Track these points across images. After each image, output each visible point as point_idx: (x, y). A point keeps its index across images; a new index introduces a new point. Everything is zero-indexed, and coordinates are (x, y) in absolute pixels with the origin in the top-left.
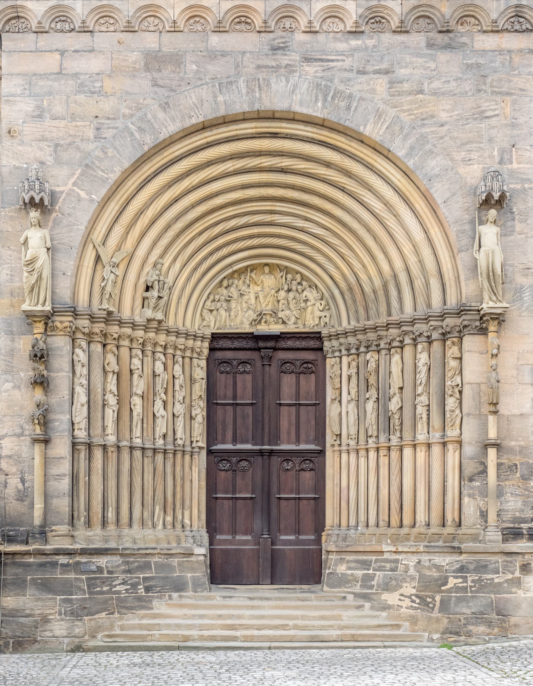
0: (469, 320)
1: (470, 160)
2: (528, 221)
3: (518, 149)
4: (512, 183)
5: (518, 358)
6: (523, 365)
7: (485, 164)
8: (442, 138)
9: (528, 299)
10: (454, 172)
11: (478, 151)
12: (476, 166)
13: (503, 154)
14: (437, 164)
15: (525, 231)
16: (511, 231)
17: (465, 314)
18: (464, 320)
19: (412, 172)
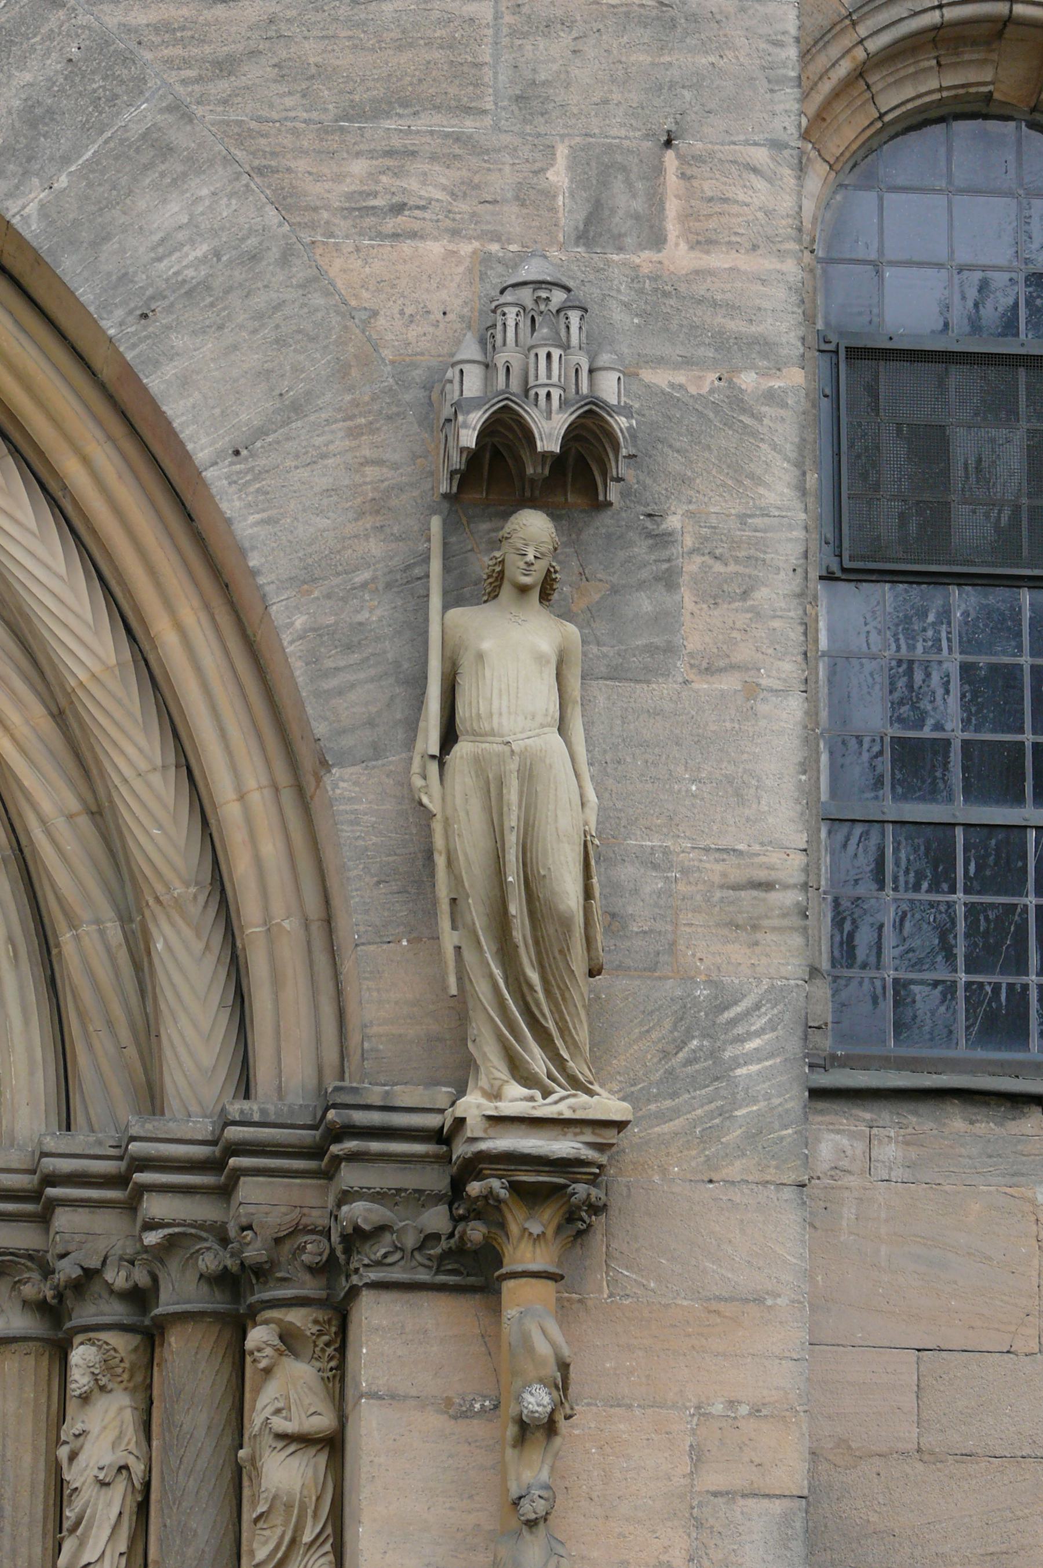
0: (379, 1197)
1: (398, 209)
2: (761, 594)
3: (699, 159)
4: (660, 362)
5: (698, 1456)
6: (728, 1495)
7: (496, 237)
8: (226, 66)
9: (763, 1076)
10: (300, 272)
11: (450, 160)
12: (434, 248)
13: (604, 183)
14: (192, 223)
15: (744, 653)
16: (651, 649)
17: (354, 1157)
18: (346, 1197)
19: (38, 259)
